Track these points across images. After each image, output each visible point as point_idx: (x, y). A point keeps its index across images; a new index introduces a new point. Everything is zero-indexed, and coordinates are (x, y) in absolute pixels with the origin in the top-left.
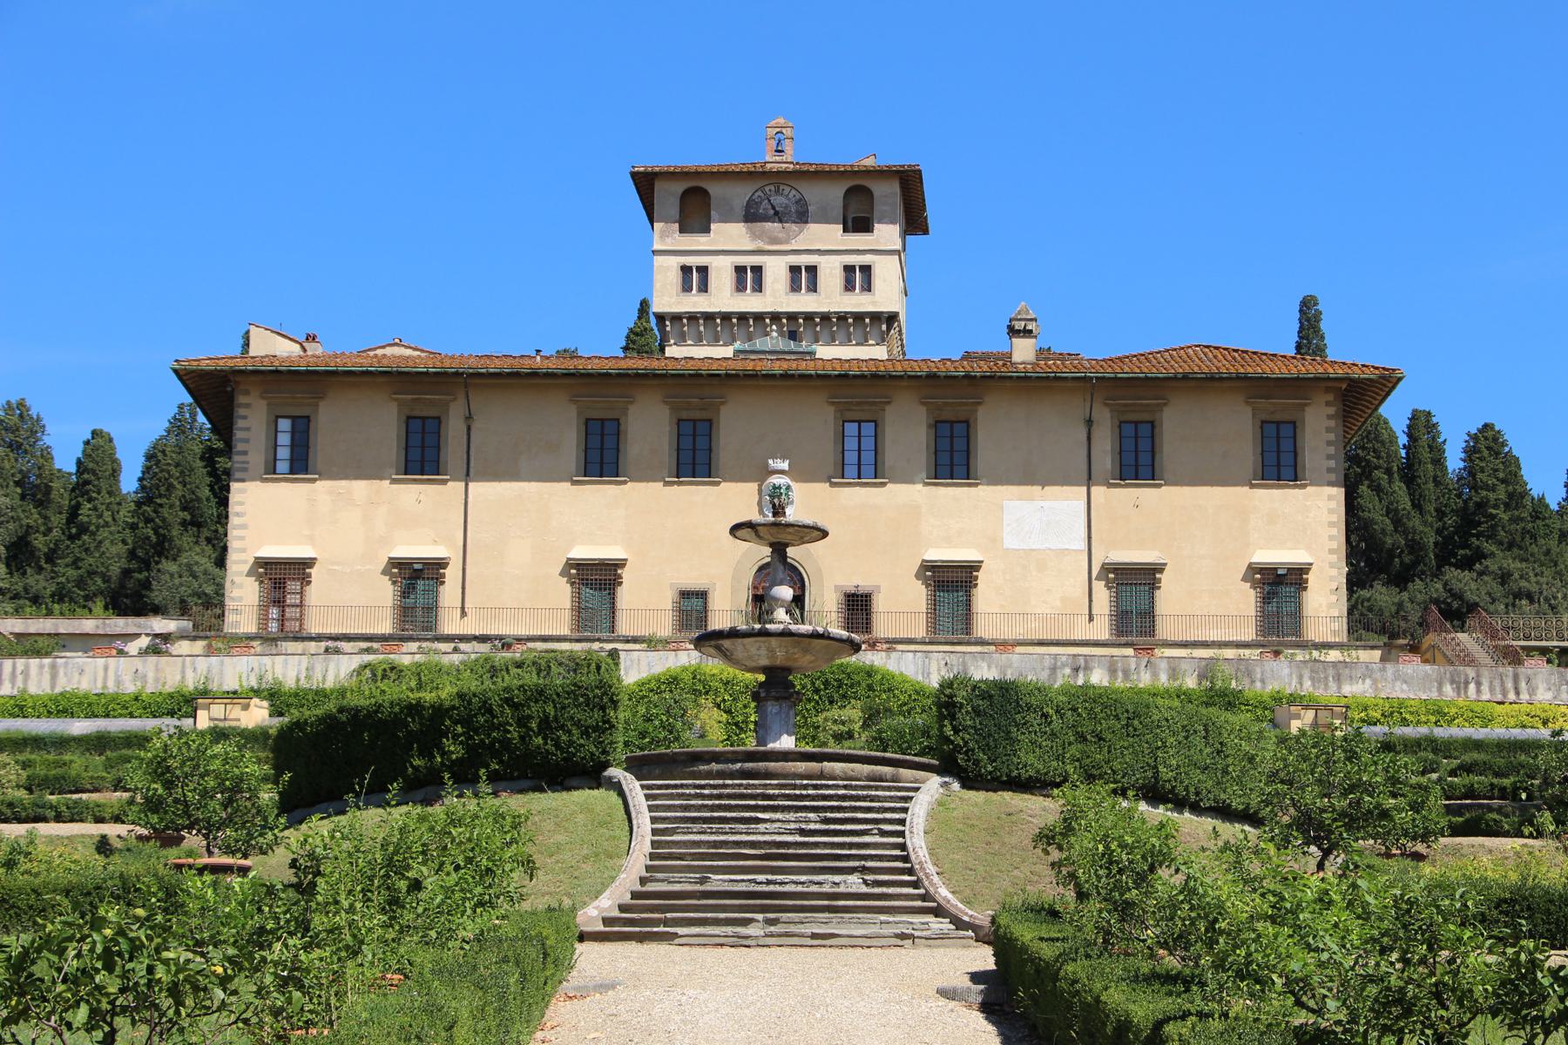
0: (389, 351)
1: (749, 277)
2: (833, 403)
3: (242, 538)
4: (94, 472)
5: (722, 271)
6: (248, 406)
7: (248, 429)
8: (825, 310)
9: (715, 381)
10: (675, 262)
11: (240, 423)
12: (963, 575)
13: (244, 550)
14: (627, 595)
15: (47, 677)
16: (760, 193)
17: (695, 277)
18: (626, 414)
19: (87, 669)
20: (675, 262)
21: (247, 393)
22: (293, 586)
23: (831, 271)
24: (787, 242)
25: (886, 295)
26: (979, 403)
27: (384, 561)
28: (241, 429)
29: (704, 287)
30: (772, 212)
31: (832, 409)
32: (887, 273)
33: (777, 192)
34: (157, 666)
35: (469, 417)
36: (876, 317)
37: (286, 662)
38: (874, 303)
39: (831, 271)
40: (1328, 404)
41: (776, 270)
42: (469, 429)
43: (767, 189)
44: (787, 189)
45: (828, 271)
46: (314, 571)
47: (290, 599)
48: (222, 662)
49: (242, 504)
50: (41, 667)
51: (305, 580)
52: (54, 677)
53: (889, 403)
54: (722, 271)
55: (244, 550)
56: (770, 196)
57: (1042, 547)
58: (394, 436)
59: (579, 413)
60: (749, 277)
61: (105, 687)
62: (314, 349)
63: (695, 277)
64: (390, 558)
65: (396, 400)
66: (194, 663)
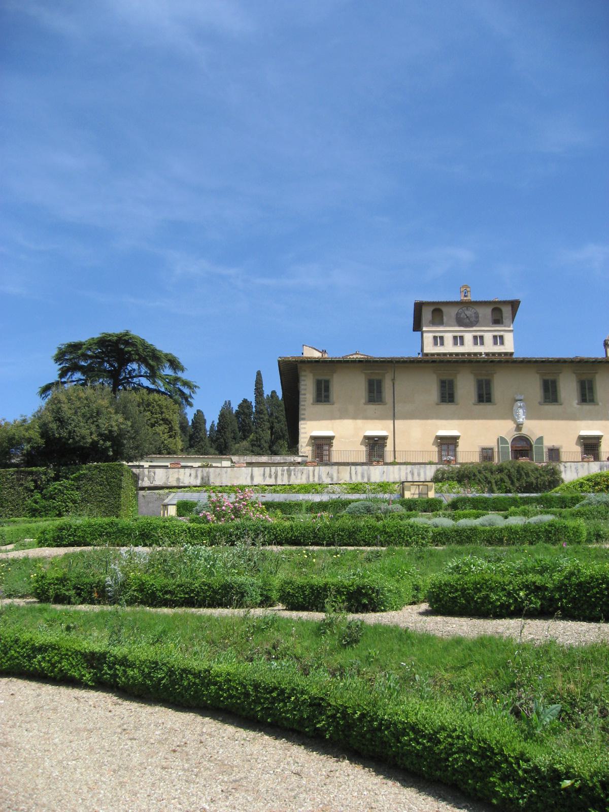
0: (355, 356)
2: (538, 373)
3: (305, 428)
4: (199, 423)
5: (449, 338)
6: (305, 376)
7: (306, 385)
8: (487, 351)
9: (492, 364)
10: (431, 335)
11: (302, 383)
12: (594, 441)
13: (306, 433)
14: (459, 449)
15: (286, 476)
17: (439, 340)
19: (305, 472)
20: (431, 335)
21: (305, 371)
22: (326, 448)
23: (488, 337)
25: (509, 346)
26: (596, 373)
27: (361, 438)
28: (303, 385)
29: (442, 344)
31: (538, 376)
32: (509, 338)
33: (467, 309)
35: (393, 380)
36: (506, 354)
37: (400, 469)
38: (505, 349)
39: (488, 337)
41: (468, 337)
42: (394, 384)
46: (334, 441)
47: (325, 453)
49: (304, 414)
50: (283, 471)
51: (330, 445)
52: (289, 475)
53: (561, 373)
54: (449, 338)
55: (306, 433)
58: (364, 387)
61: (314, 481)
62: (326, 356)
64: (364, 436)
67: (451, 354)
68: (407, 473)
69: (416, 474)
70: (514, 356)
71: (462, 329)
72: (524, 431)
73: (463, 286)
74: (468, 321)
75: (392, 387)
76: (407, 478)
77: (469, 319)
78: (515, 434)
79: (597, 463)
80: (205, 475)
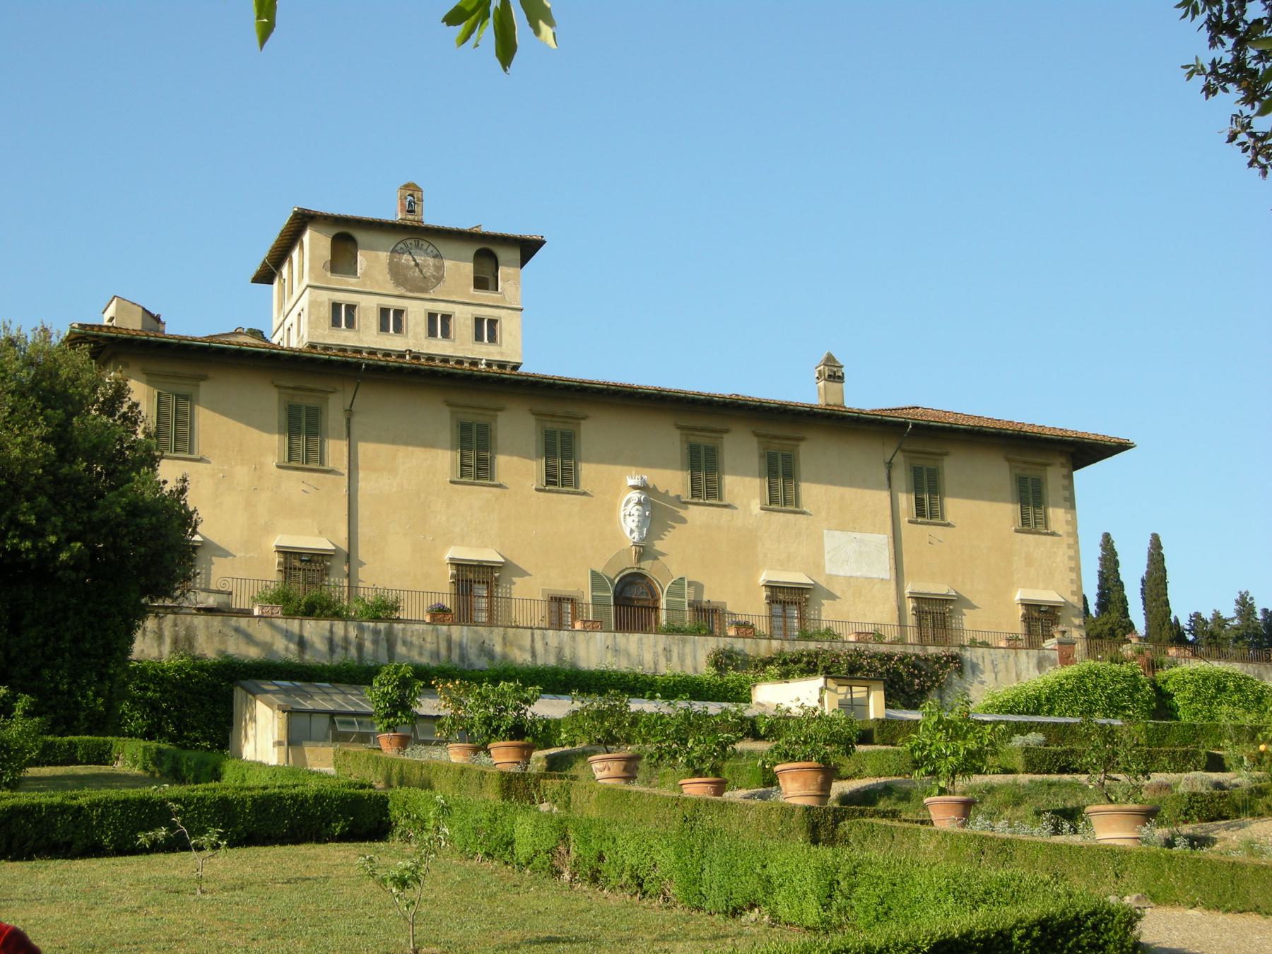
1: (391, 319)
8: (460, 354)
16: (402, 245)
18: (496, 421)
24: (425, 290)
30: (413, 263)
33: (417, 246)
34: (504, 638)
35: (349, 413)
38: (502, 354)
39: (463, 318)
40: (1063, 465)
41: (416, 312)
42: (349, 420)
43: (408, 242)
44: (426, 245)
45: (462, 320)
48: (641, 639)
56: (411, 249)
57: (859, 574)
60: (391, 319)
63: (343, 315)
66: (544, 637)
67: (372, 352)
68: (656, 654)
69: (675, 658)
70: (521, 370)
71: (401, 291)
72: (647, 566)
73: (407, 187)
74: (417, 273)
75: (345, 429)
76: (656, 664)
77: (421, 271)
78: (629, 563)
79: (1034, 653)
80: (183, 633)
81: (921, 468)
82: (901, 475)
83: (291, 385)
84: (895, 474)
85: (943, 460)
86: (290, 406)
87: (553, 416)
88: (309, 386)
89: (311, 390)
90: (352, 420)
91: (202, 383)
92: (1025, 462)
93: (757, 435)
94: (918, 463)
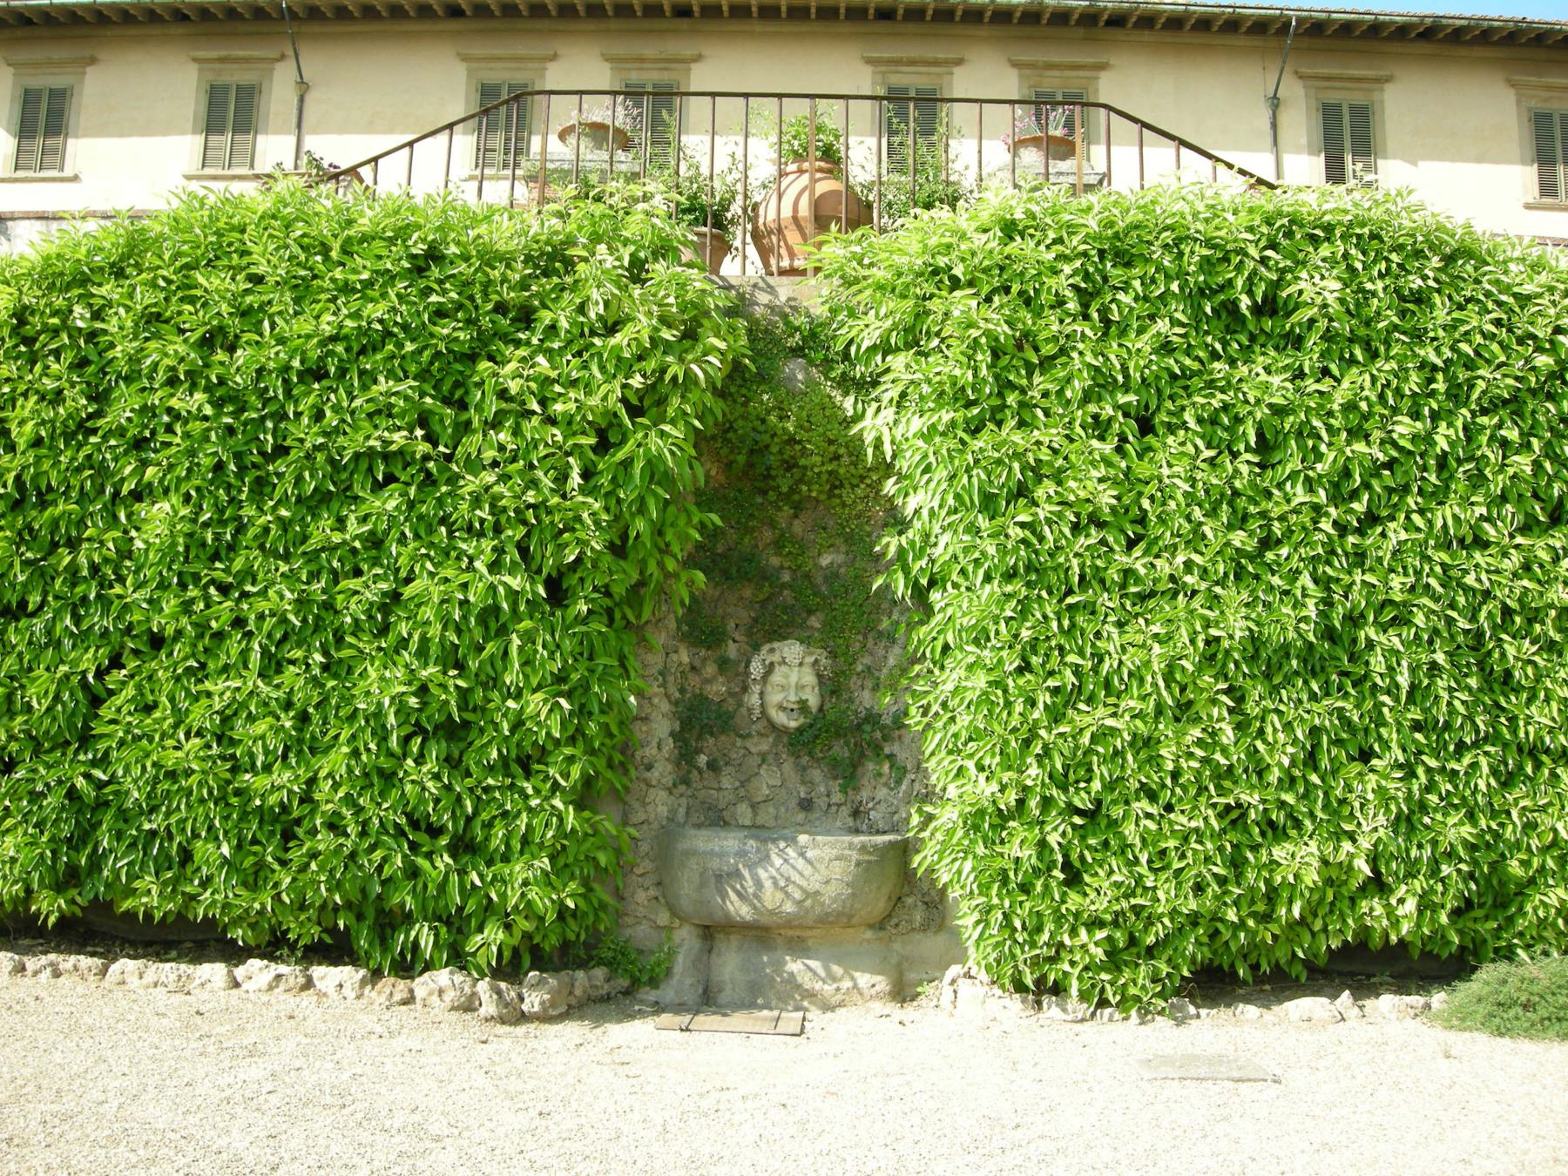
35: (303, 87)
42: (302, 100)
59: (469, 76)
65: (195, 60)
75: (295, 112)
81: (1340, 105)
82: (1299, 121)
83: (214, 54)
84: (1285, 118)
85: (1382, 90)
86: (212, 87)
87: (642, 60)
88: (241, 53)
89: (246, 60)
90: (308, 99)
91: (89, 70)
92: (1548, 88)
93: (1015, 64)
94: (1333, 97)
